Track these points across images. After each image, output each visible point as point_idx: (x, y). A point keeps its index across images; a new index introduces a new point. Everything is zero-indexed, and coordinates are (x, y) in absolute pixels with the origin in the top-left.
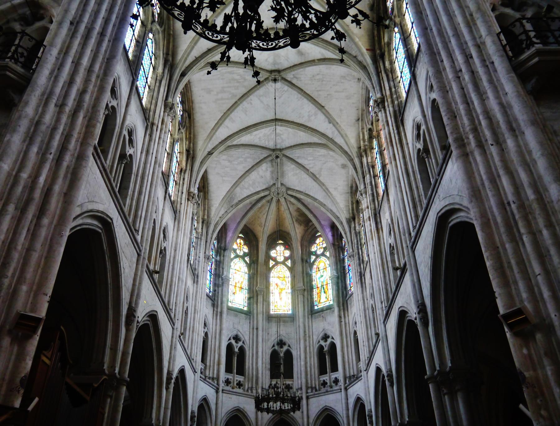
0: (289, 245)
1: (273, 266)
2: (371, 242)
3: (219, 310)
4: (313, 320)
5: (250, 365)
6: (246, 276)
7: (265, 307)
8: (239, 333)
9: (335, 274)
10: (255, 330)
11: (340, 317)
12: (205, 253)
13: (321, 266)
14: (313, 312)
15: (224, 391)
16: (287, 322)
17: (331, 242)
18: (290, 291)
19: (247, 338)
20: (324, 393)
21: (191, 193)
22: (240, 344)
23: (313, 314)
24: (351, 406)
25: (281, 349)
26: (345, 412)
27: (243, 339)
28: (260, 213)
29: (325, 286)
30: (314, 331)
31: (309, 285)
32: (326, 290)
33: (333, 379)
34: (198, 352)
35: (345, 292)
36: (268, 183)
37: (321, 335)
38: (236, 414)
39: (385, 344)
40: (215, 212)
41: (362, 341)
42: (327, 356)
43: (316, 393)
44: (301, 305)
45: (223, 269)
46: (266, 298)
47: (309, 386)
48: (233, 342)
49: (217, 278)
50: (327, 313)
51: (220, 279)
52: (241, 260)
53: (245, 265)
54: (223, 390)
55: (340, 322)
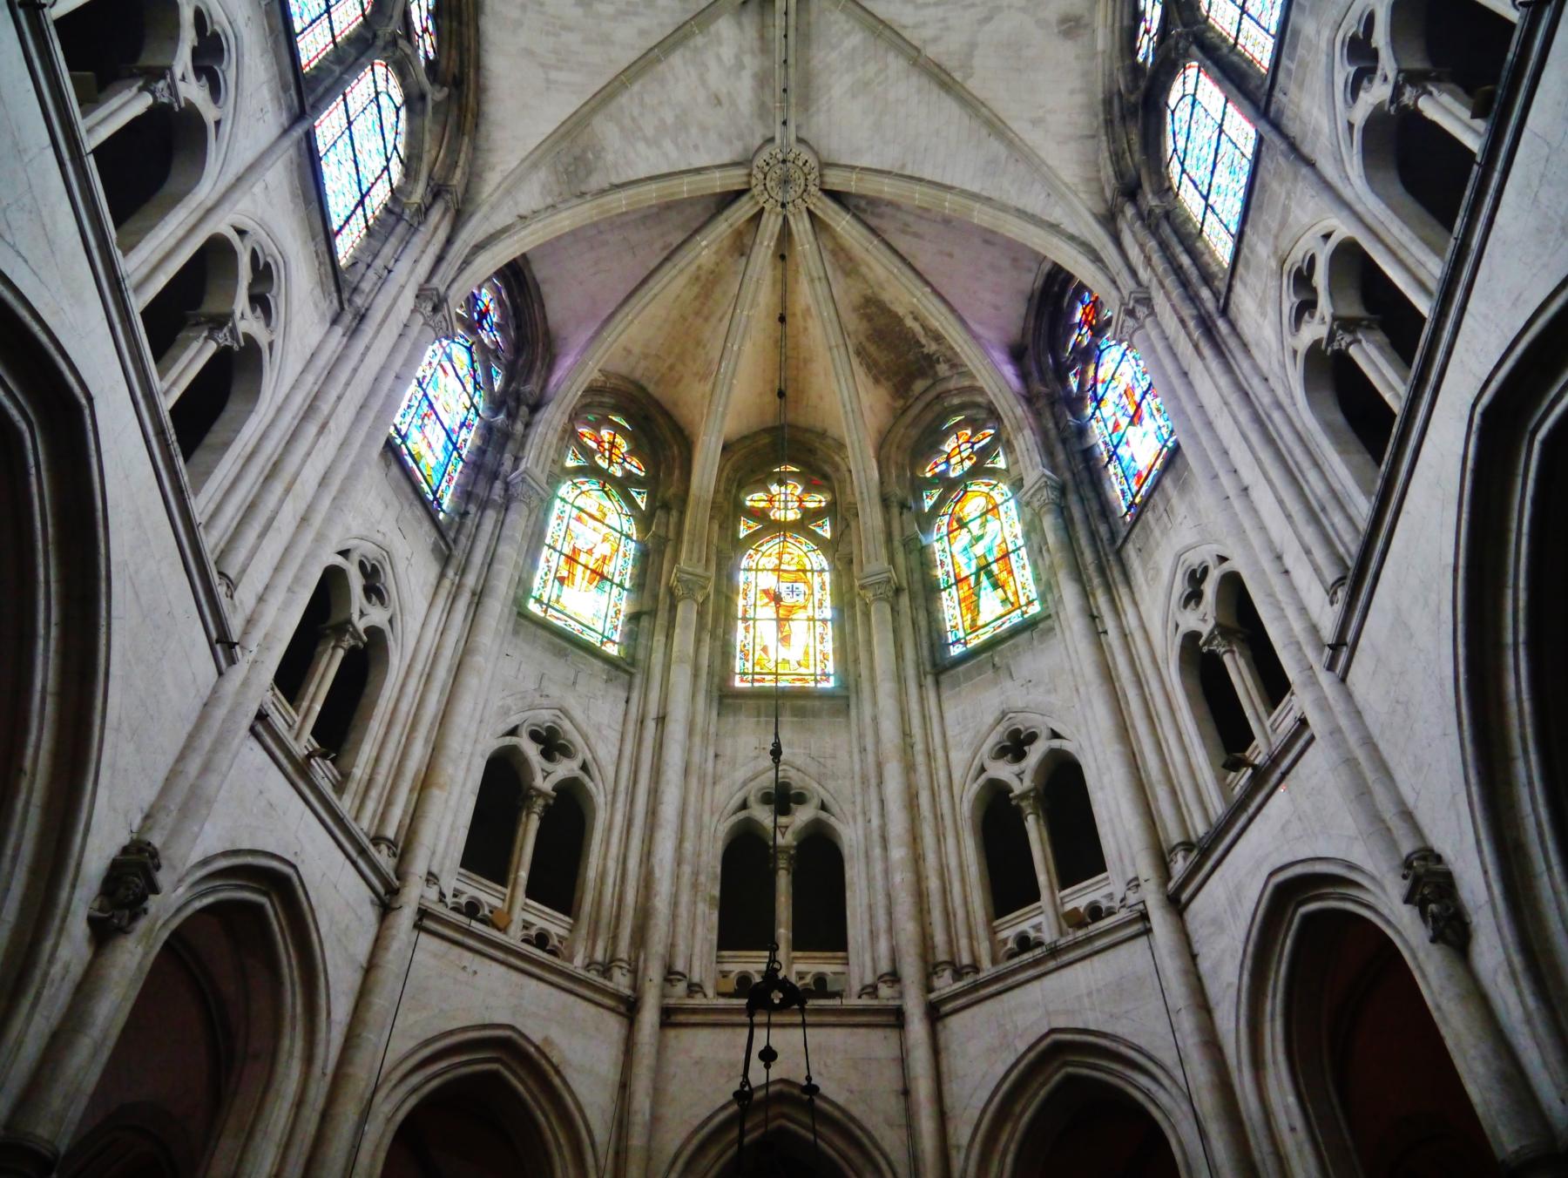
0: (825, 477)
1: (753, 537)
3: (471, 580)
4: (944, 696)
5: (611, 865)
10: (651, 725)
15: (428, 923)
16: (815, 714)
18: (828, 613)
19: (606, 753)
25: (782, 820)
27: (583, 753)
28: (707, 319)
29: (994, 567)
30: (949, 733)
31: (917, 576)
35: (1103, 530)
36: (740, 137)
38: (495, 1075)
47: (942, 955)
50: (1016, 646)
51: (498, 485)
54: (423, 913)
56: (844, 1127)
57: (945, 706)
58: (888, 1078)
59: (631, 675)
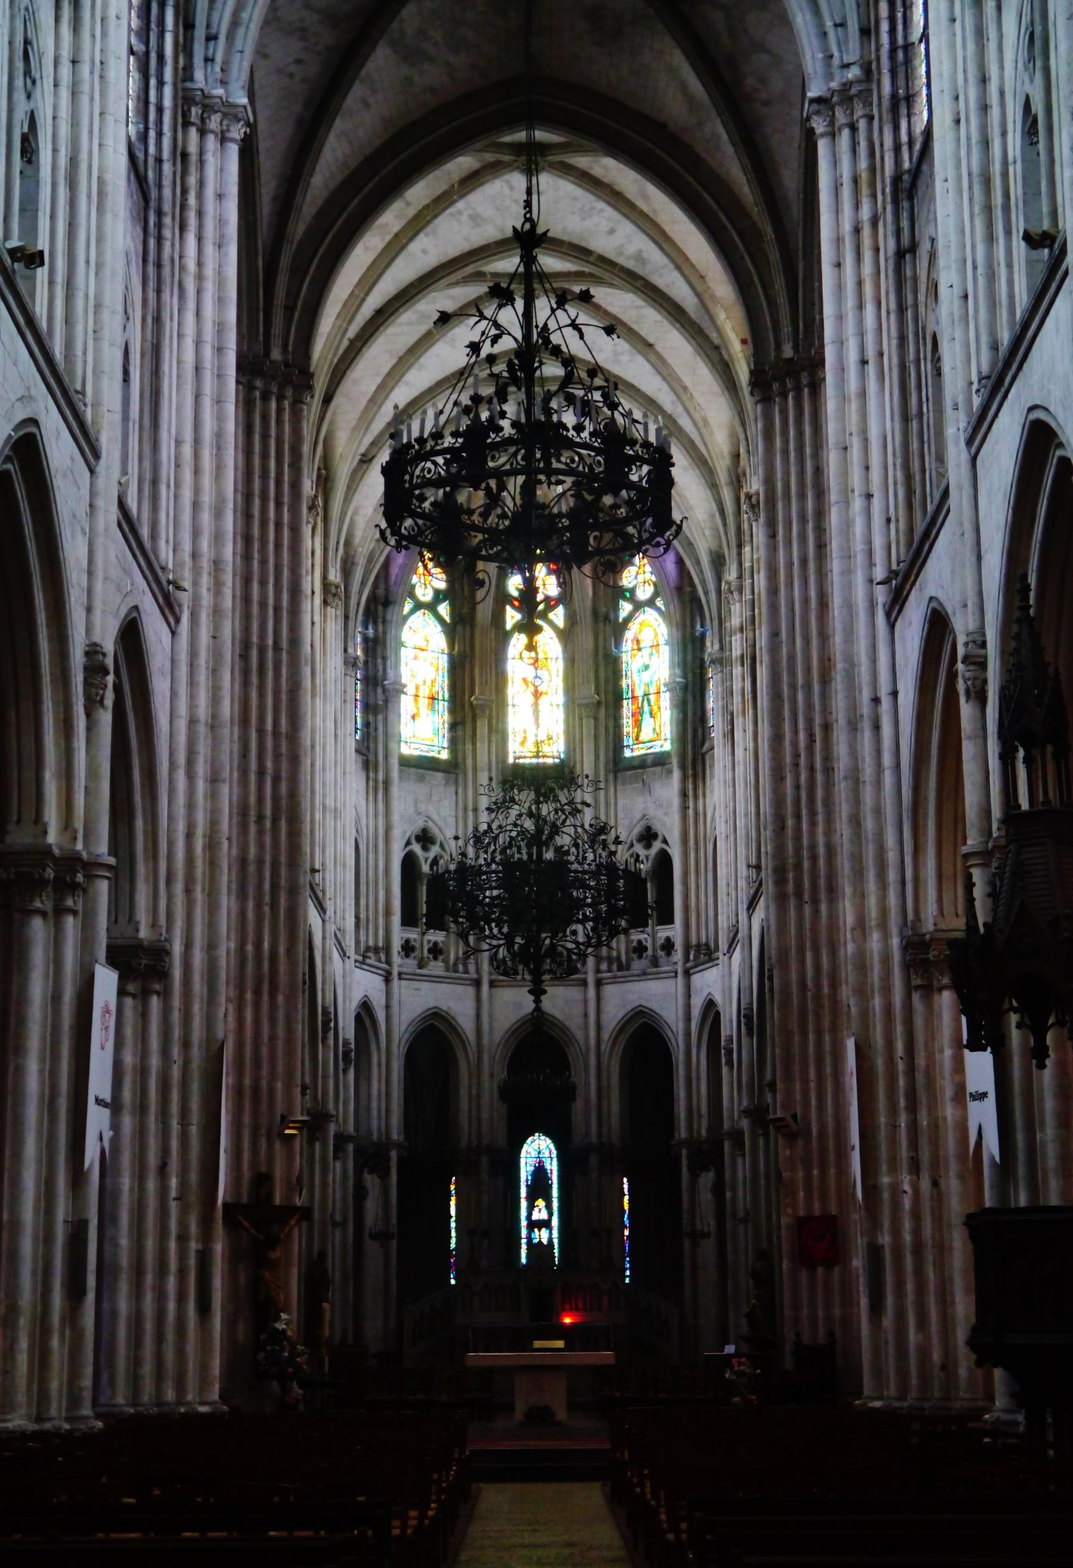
2: (741, 720)
3: (381, 776)
4: (619, 788)
6: (444, 662)
7: (493, 748)
8: (431, 824)
9: (679, 680)
10: (470, 814)
11: (684, 795)
12: (346, 650)
13: (646, 640)
17: (672, 585)
20: (638, 975)
21: (331, 584)
22: (435, 850)
23: (620, 771)
24: (696, 1012)
26: (681, 1025)
27: (440, 837)
29: (652, 698)
30: (621, 815)
31: (611, 686)
32: (655, 708)
33: (660, 942)
34: (348, 907)
35: (700, 732)
37: (637, 830)
39: (747, 953)
40: (364, 531)
41: (724, 883)
42: (649, 885)
43: (620, 974)
44: (588, 747)
45: (384, 659)
46: (497, 724)
48: (416, 848)
49: (370, 688)
51: (379, 690)
53: (439, 628)
54: (400, 974)
55: (684, 808)
56: (563, 1029)
57: (619, 795)
58: (578, 1010)
59: (457, 775)
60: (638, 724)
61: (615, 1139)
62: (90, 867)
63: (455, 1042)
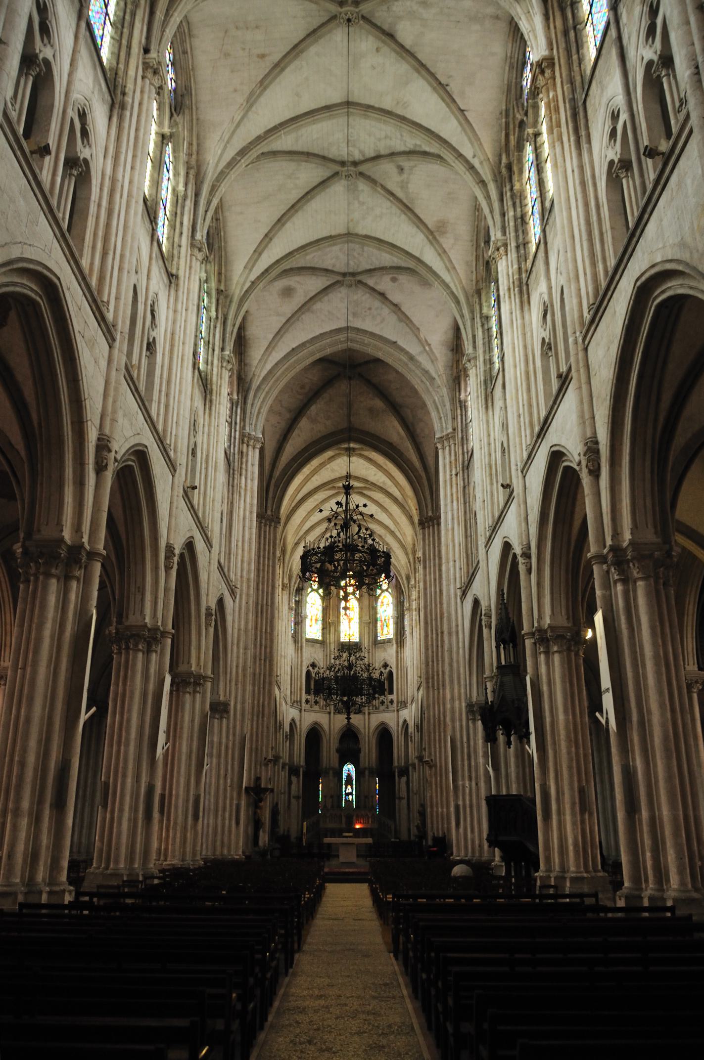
6: (320, 608)
11: (397, 652)
14: (376, 643)
22: (316, 669)
24: (401, 723)
27: (318, 665)
44: (366, 636)
48: (311, 668)
52: (316, 593)
53: (319, 597)
55: (397, 656)
56: (358, 729)
58: (362, 722)
60: (382, 629)
61: (374, 765)
62: (164, 634)
63: (322, 733)
